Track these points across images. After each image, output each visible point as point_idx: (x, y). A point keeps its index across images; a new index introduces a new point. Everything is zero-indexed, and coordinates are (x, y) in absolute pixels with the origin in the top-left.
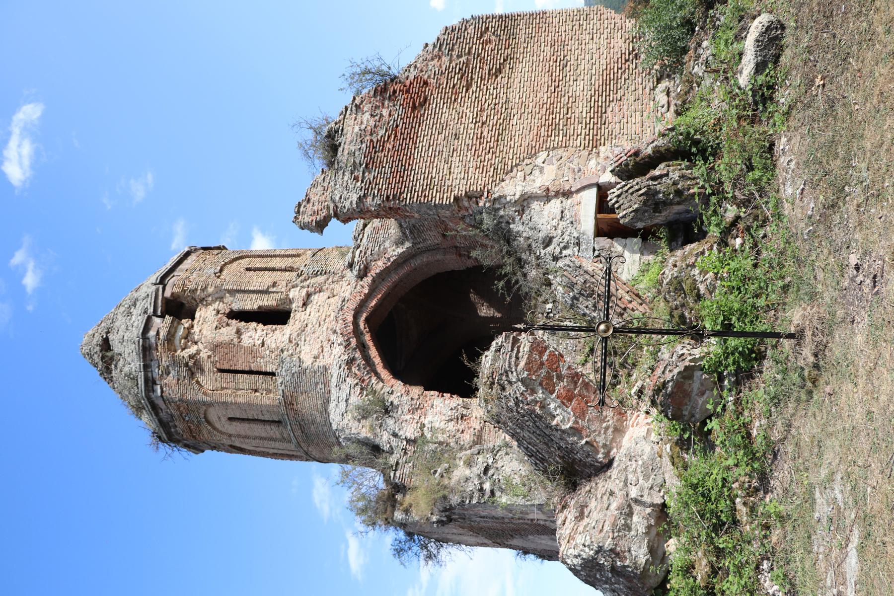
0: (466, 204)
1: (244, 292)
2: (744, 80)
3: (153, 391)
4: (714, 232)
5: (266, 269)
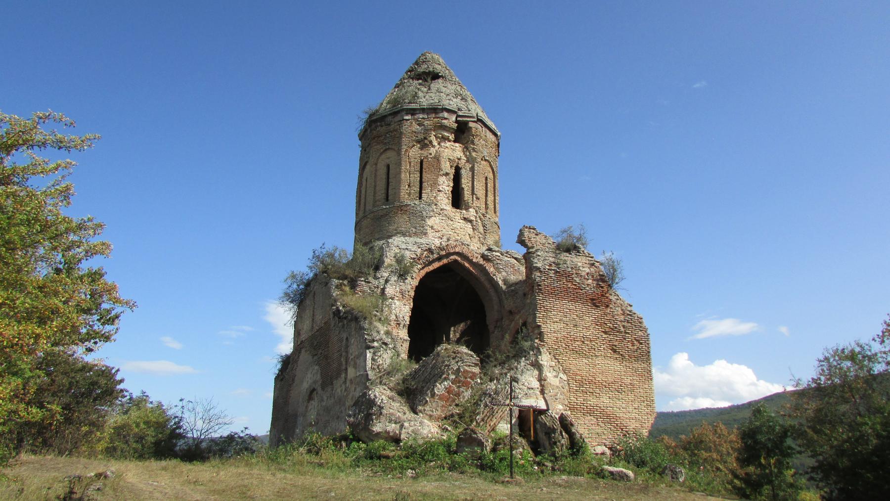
0: (536, 332)
2: (606, 467)
3: (407, 114)
4: (537, 459)
5: (487, 191)
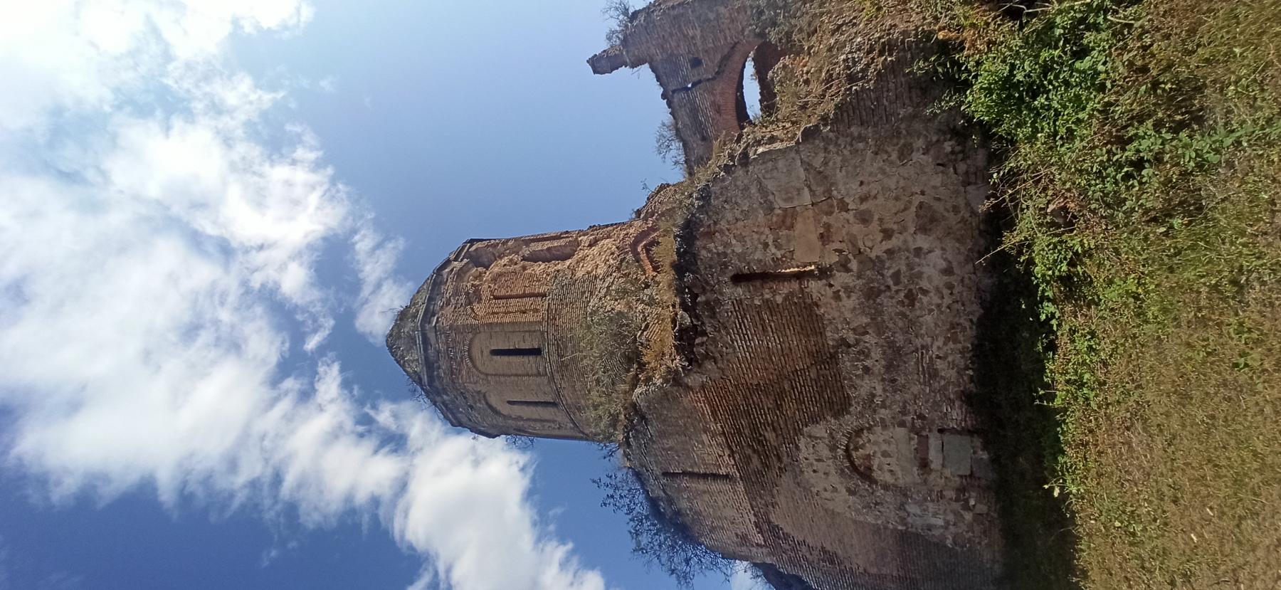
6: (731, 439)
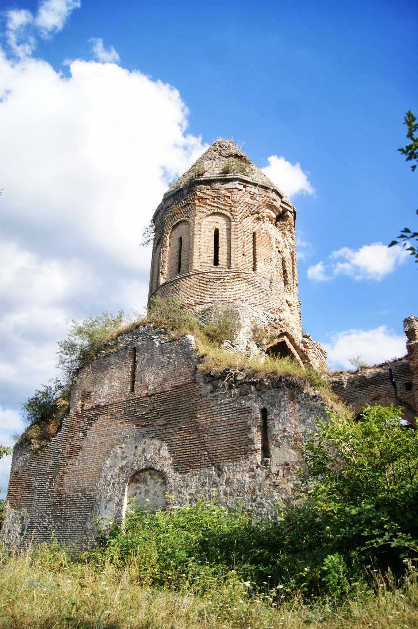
1: (293, 263)
6: (158, 396)
